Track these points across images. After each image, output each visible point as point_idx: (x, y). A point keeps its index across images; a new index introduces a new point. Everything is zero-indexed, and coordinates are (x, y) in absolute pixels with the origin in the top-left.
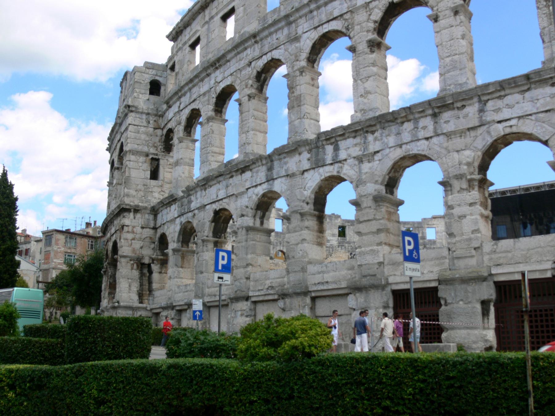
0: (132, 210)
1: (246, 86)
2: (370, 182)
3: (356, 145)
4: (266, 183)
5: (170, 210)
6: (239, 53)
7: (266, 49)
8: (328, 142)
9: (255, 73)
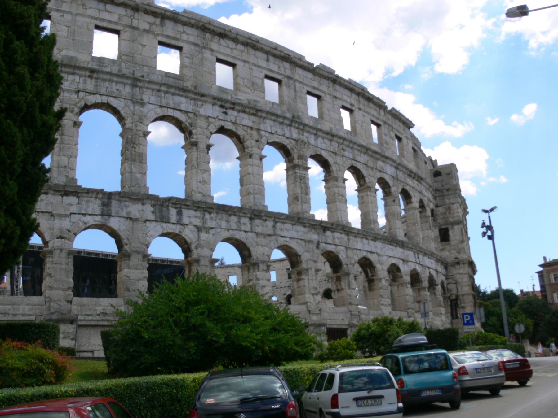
3: (196, 217)
8: (174, 206)
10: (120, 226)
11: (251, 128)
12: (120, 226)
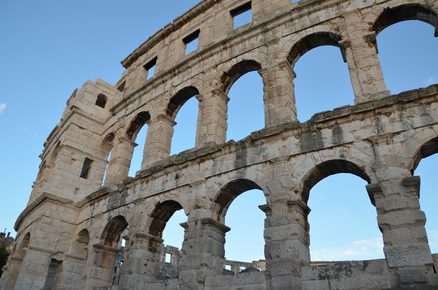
2: (393, 165)
4: (235, 171)
5: (98, 206)
6: (203, 59)
7: (237, 53)
8: (326, 125)
9: (221, 73)
10: (257, 175)
12: (257, 175)
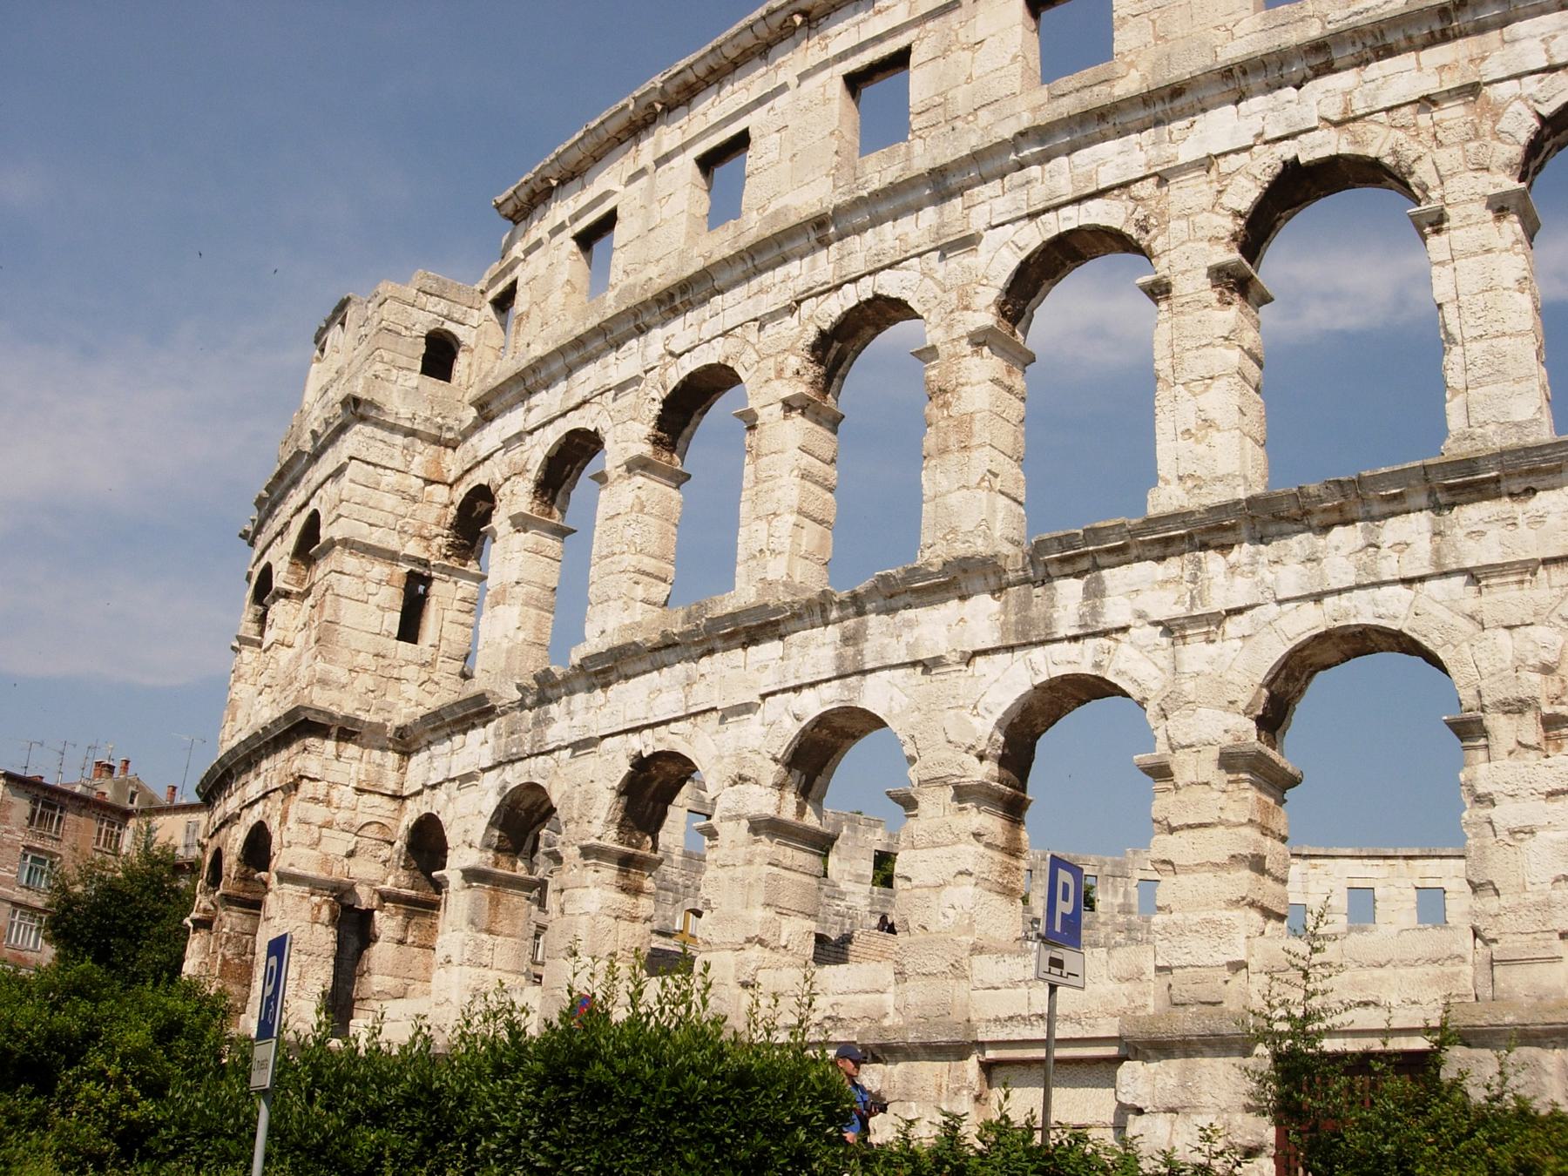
0: (334, 731)
1: (780, 373)
2: (1209, 705)
4: (836, 683)
6: (758, 271)
7: (857, 265)
8: (1068, 570)
9: (811, 335)
11: (1428, 102)
